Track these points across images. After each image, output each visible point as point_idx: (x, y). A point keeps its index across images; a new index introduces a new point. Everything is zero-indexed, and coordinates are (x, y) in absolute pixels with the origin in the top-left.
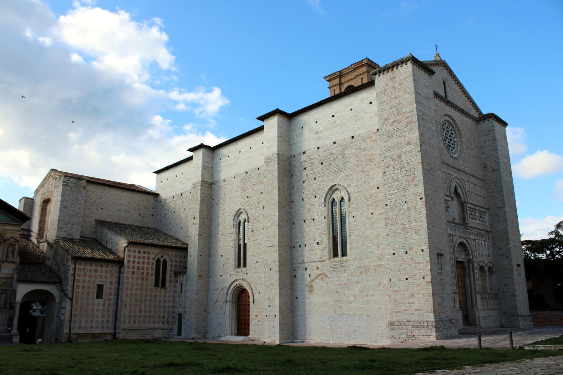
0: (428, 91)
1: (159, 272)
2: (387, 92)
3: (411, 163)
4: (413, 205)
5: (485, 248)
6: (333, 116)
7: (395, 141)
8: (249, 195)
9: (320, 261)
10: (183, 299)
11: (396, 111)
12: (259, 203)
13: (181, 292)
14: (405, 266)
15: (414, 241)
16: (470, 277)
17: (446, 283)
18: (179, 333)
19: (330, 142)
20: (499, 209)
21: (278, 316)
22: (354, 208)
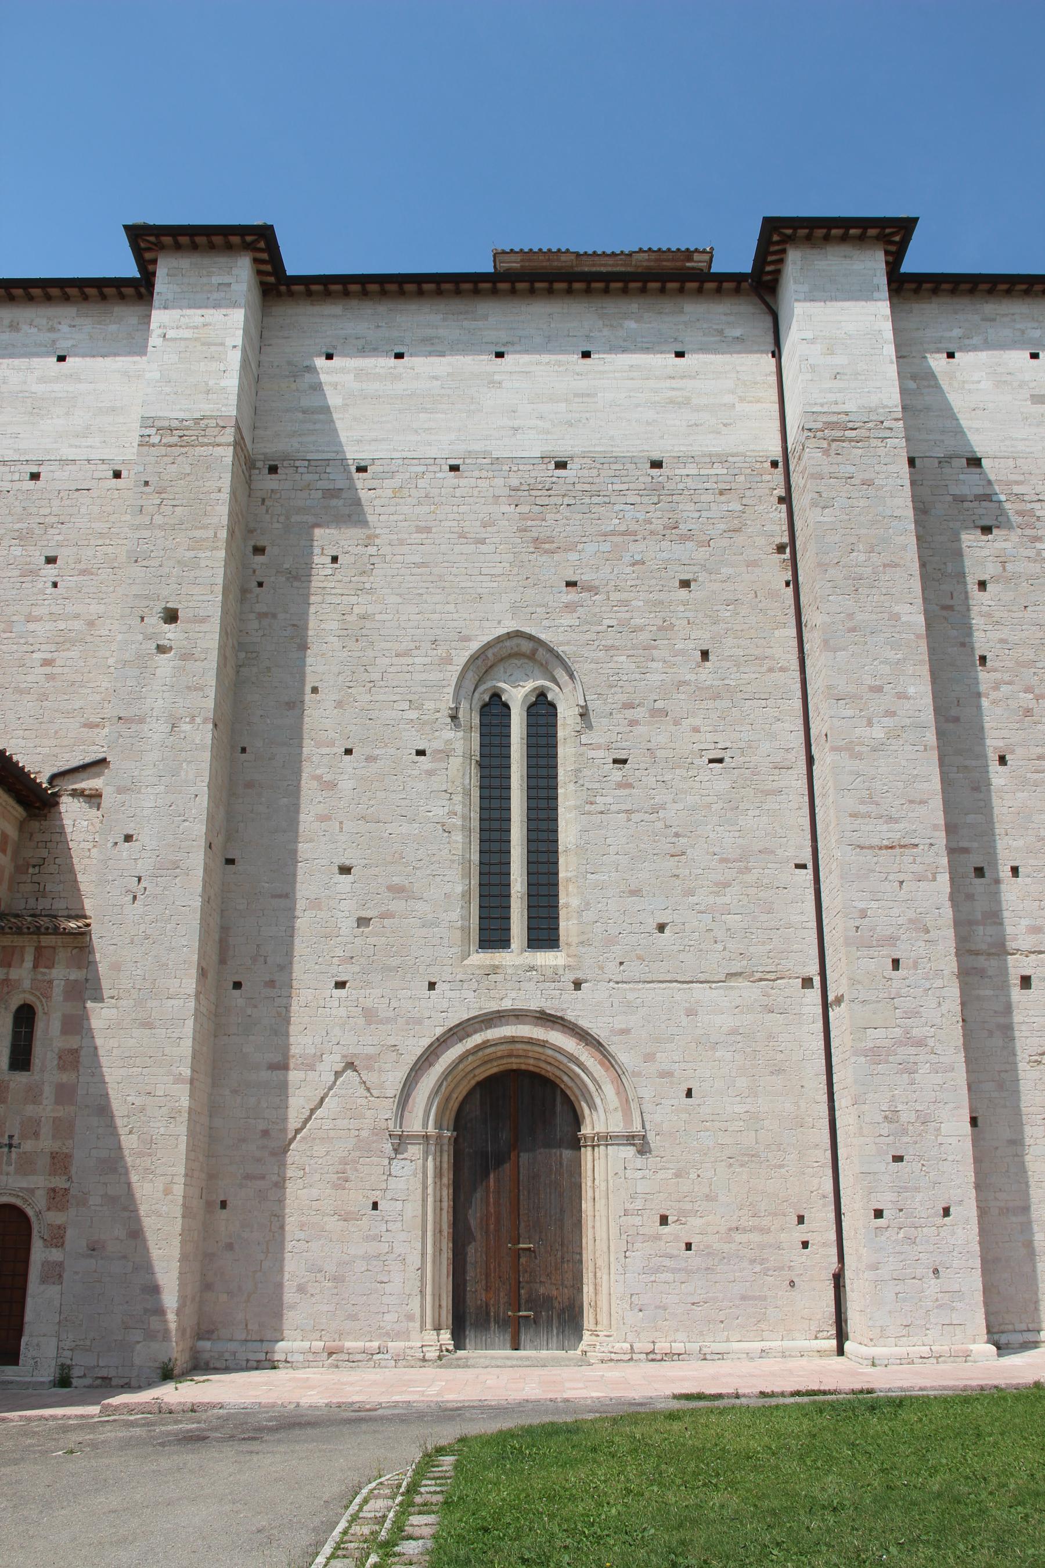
8: (584, 576)
10: (47, 1109)
12: (666, 628)
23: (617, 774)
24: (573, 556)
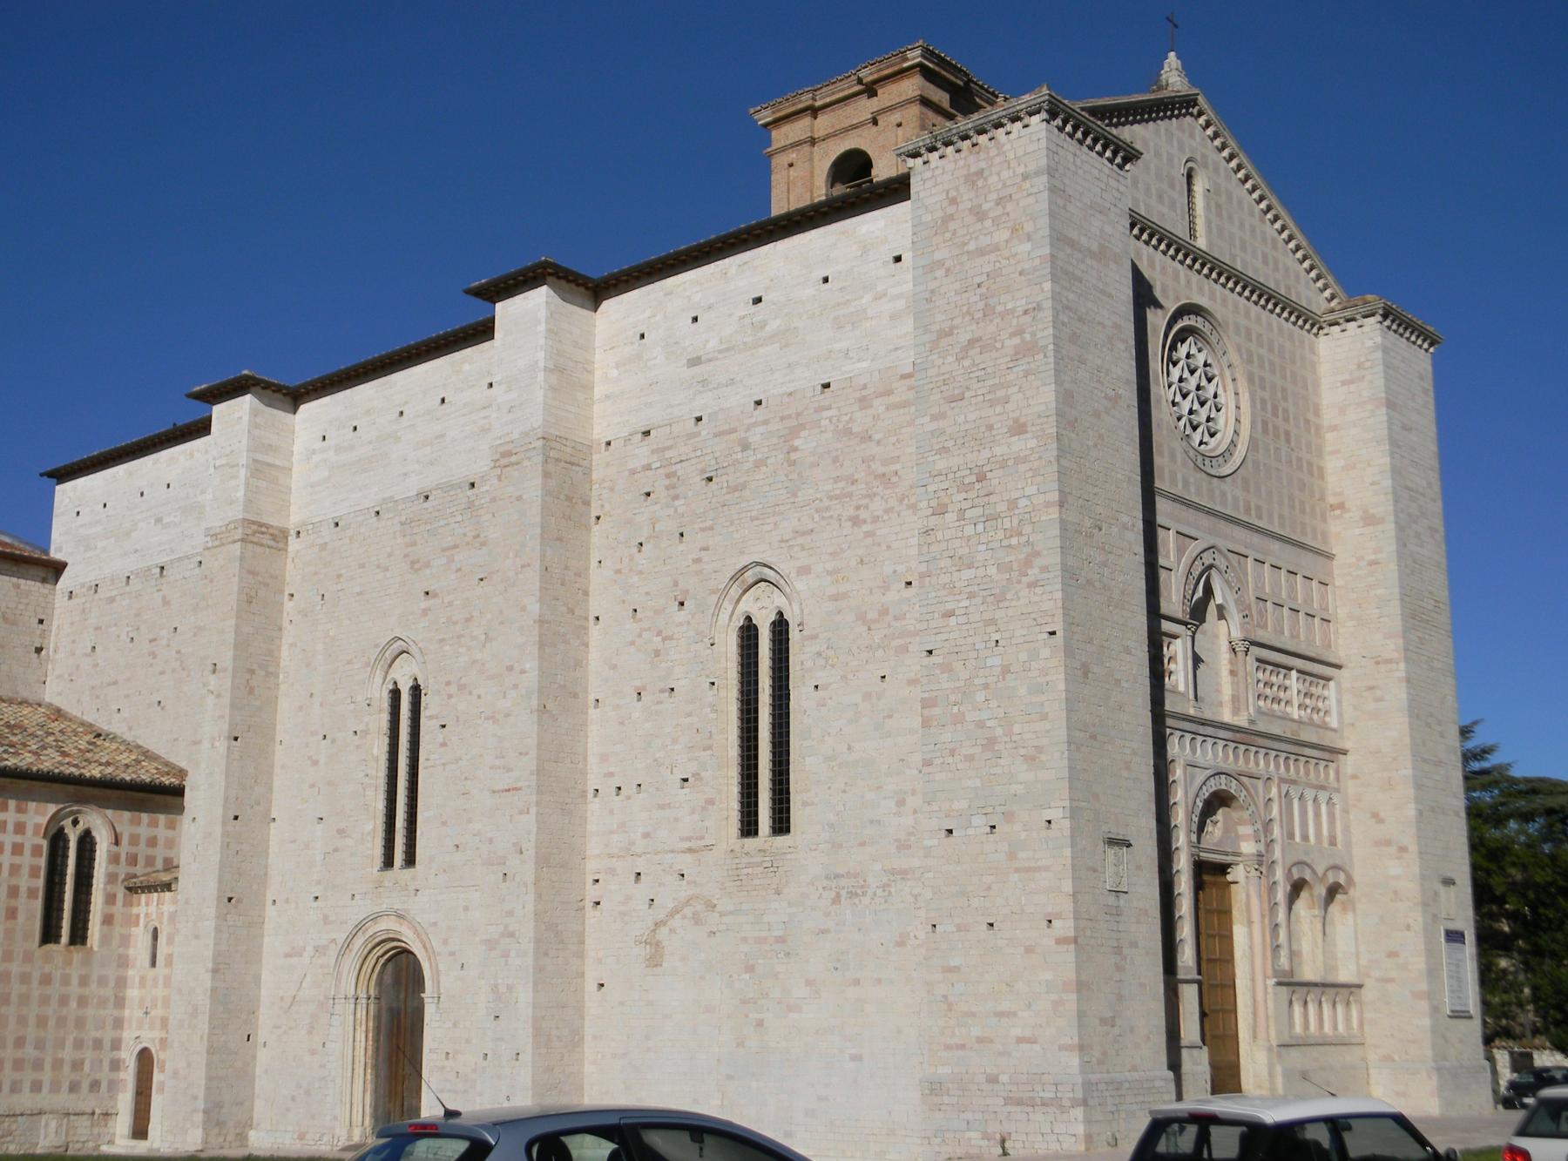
0: (1109, 229)
1: (63, 883)
2: (952, 226)
3: (1022, 503)
4: (1023, 657)
5: (1317, 815)
6: (758, 300)
7: (971, 417)
9: (690, 850)
11: (981, 305)
13: (153, 964)
14: (988, 880)
15: (1020, 789)
16: (1250, 923)
17: (1134, 944)
18: (140, 1132)
19: (738, 400)
20: (1382, 667)
21: (527, 1057)
22: (819, 654)
23: (441, 736)
24: (428, 572)
